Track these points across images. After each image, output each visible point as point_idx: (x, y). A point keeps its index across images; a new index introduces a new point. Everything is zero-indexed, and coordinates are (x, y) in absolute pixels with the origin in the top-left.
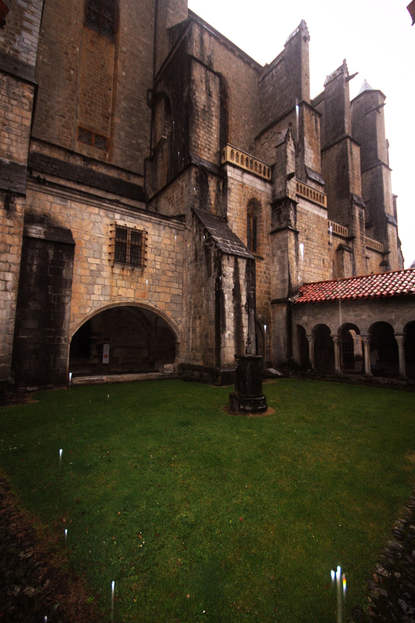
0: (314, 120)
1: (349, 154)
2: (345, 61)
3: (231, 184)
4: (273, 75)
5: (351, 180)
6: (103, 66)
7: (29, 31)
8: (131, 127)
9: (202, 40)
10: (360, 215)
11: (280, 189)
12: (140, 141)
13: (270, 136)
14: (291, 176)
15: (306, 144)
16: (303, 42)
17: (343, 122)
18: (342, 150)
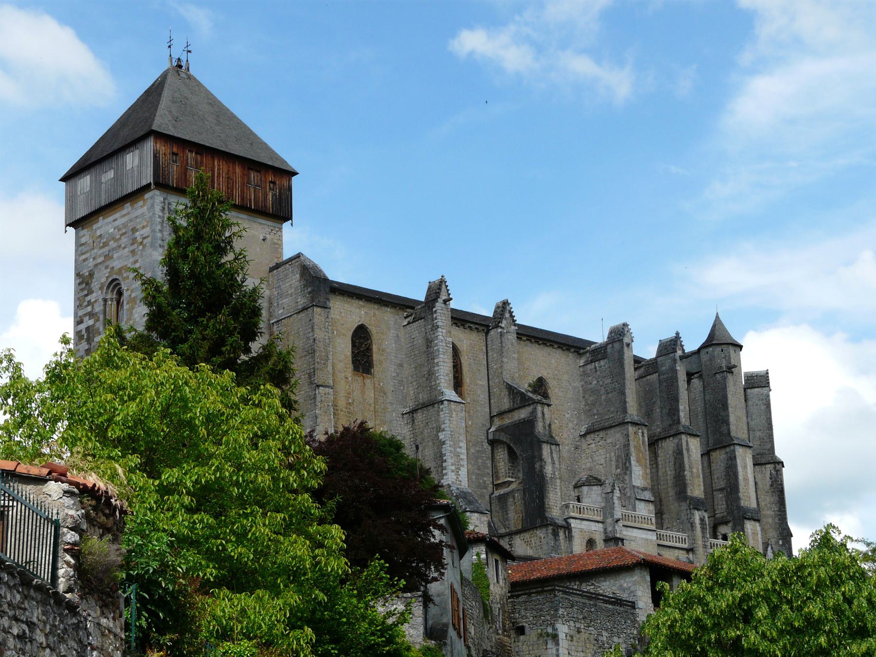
0: (640, 434)
1: (685, 452)
2: (677, 334)
3: (575, 533)
4: (595, 368)
5: (688, 482)
6: (180, 67)
7: (463, 466)
8: (479, 469)
9: (543, 414)
10: (702, 520)
11: (610, 529)
12: (485, 479)
13: (597, 439)
14: (617, 521)
15: (633, 463)
16: (625, 348)
17: (678, 410)
18: (677, 446)
